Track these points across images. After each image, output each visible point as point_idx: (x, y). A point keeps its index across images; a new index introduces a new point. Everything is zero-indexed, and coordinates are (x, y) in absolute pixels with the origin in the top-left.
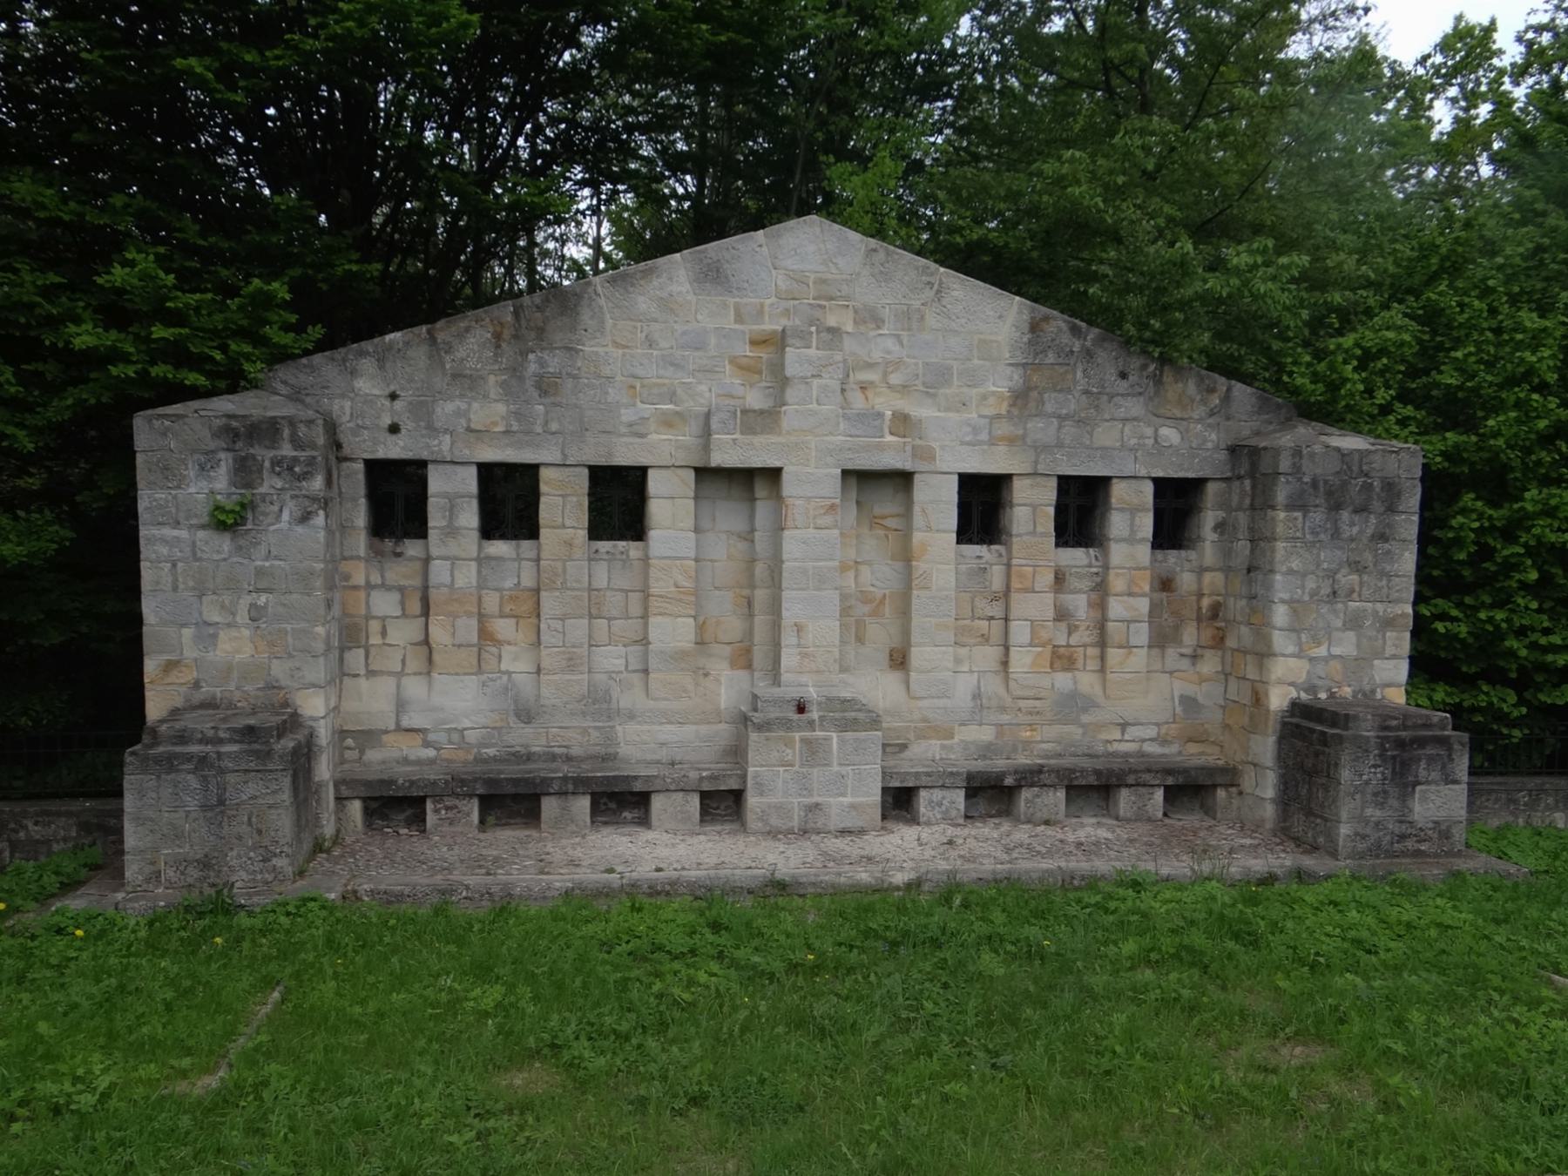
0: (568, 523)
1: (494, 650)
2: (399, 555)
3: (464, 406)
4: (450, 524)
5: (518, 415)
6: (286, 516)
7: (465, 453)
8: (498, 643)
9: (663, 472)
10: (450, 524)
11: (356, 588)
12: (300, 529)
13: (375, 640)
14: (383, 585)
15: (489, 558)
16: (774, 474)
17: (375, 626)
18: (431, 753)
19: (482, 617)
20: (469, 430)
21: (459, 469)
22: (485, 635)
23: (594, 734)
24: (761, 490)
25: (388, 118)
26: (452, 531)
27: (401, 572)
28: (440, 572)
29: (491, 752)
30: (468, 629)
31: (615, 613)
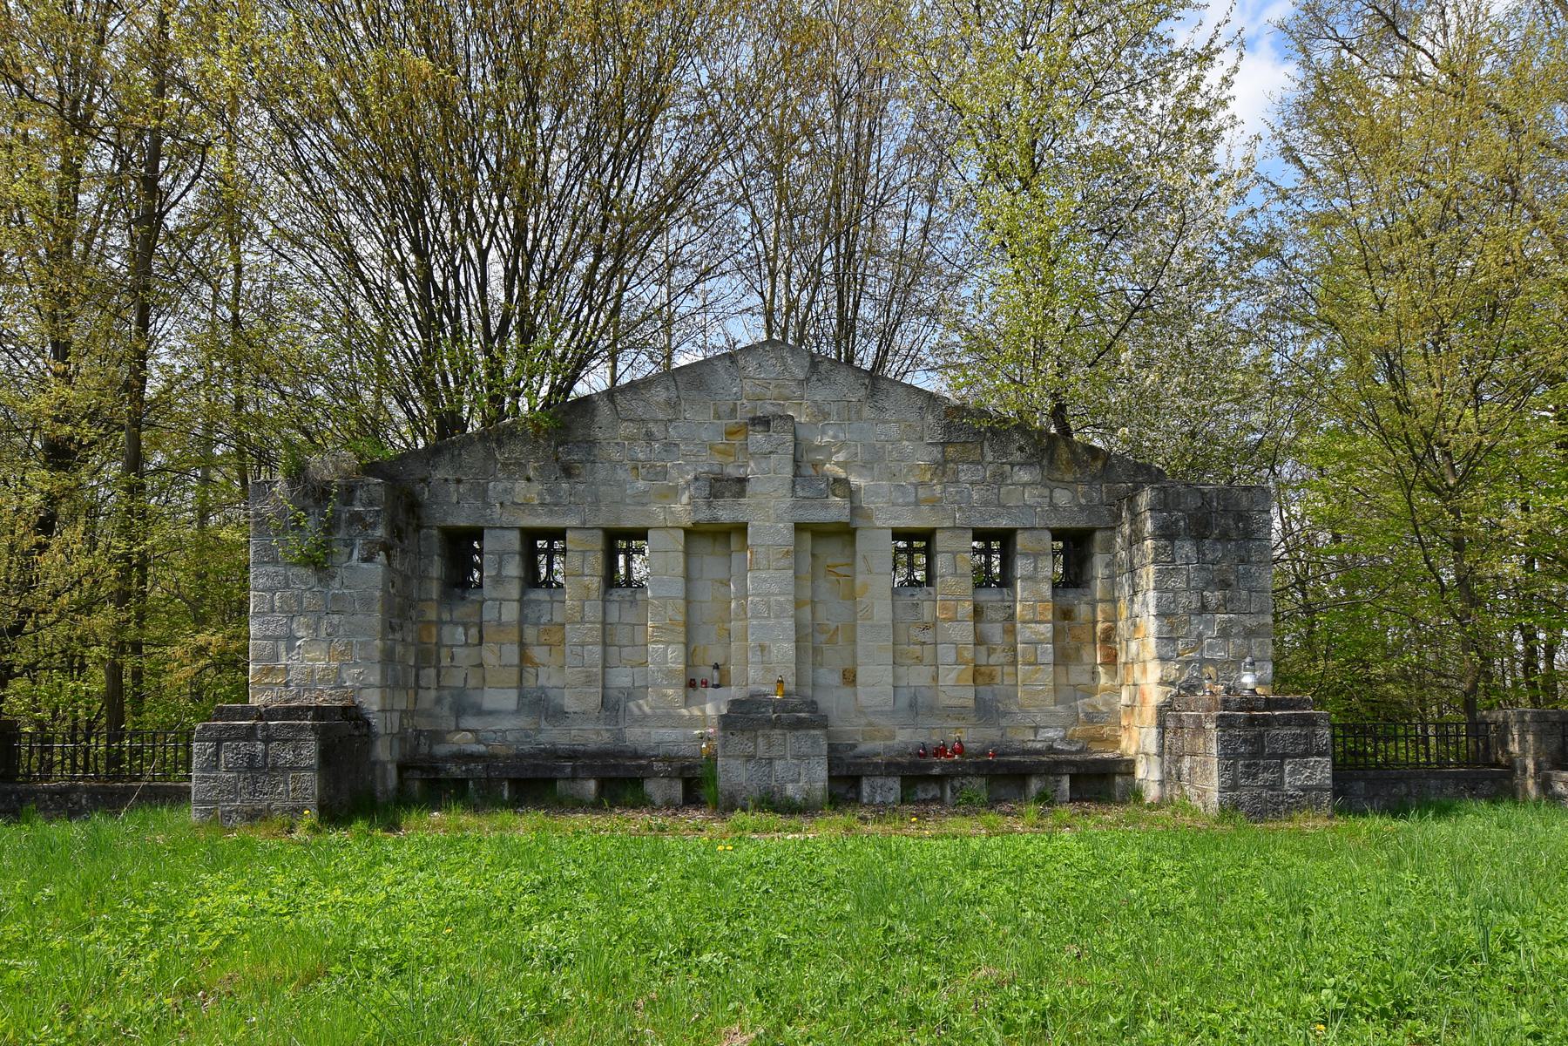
0: (587, 571)
1: (533, 670)
2: (463, 599)
3: (509, 485)
4: (499, 574)
5: (549, 491)
6: (356, 555)
7: (506, 519)
8: (536, 665)
9: (663, 532)
10: (499, 574)
11: (429, 622)
12: (365, 565)
13: (445, 662)
14: (451, 621)
15: (531, 601)
16: (742, 529)
17: (444, 652)
18: (482, 748)
19: (522, 645)
20: (514, 503)
21: (506, 532)
22: (524, 658)
23: (606, 735)
24: (735, 542)
25: (413, 178)
26: (499, 579)
27: (461, 611)
28: (489, 614)
29: (526, 747)
30: (511, 654)
31: (625, 642)
